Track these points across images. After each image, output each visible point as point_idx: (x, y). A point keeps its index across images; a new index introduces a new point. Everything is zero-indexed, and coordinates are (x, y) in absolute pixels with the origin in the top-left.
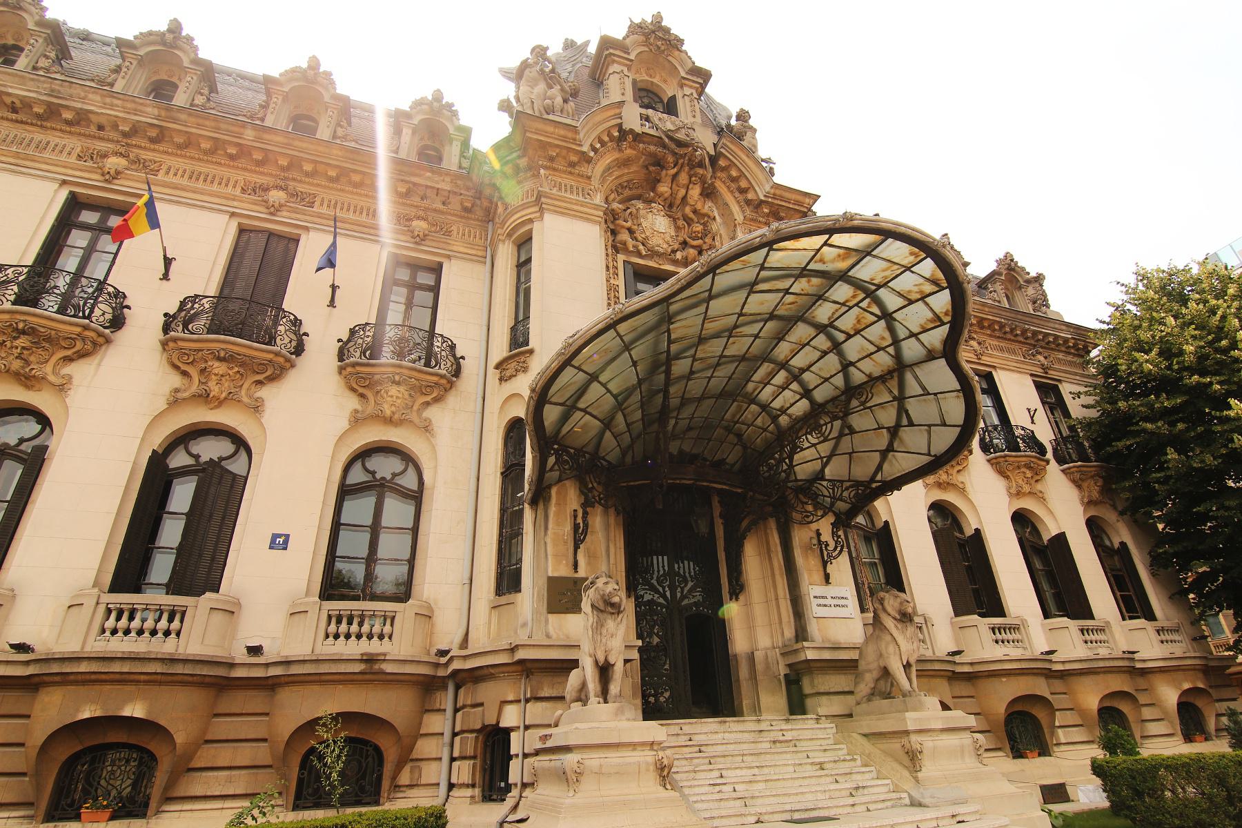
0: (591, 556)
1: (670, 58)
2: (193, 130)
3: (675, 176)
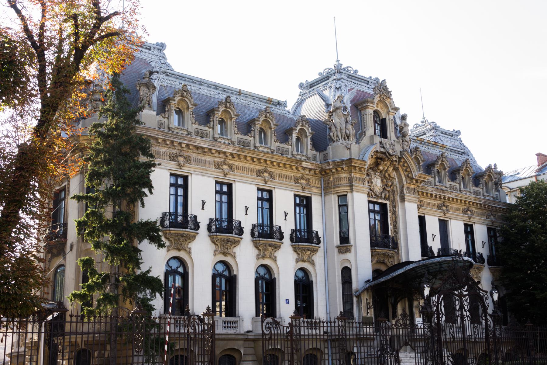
1: (386, 102)
2: (247, 155)
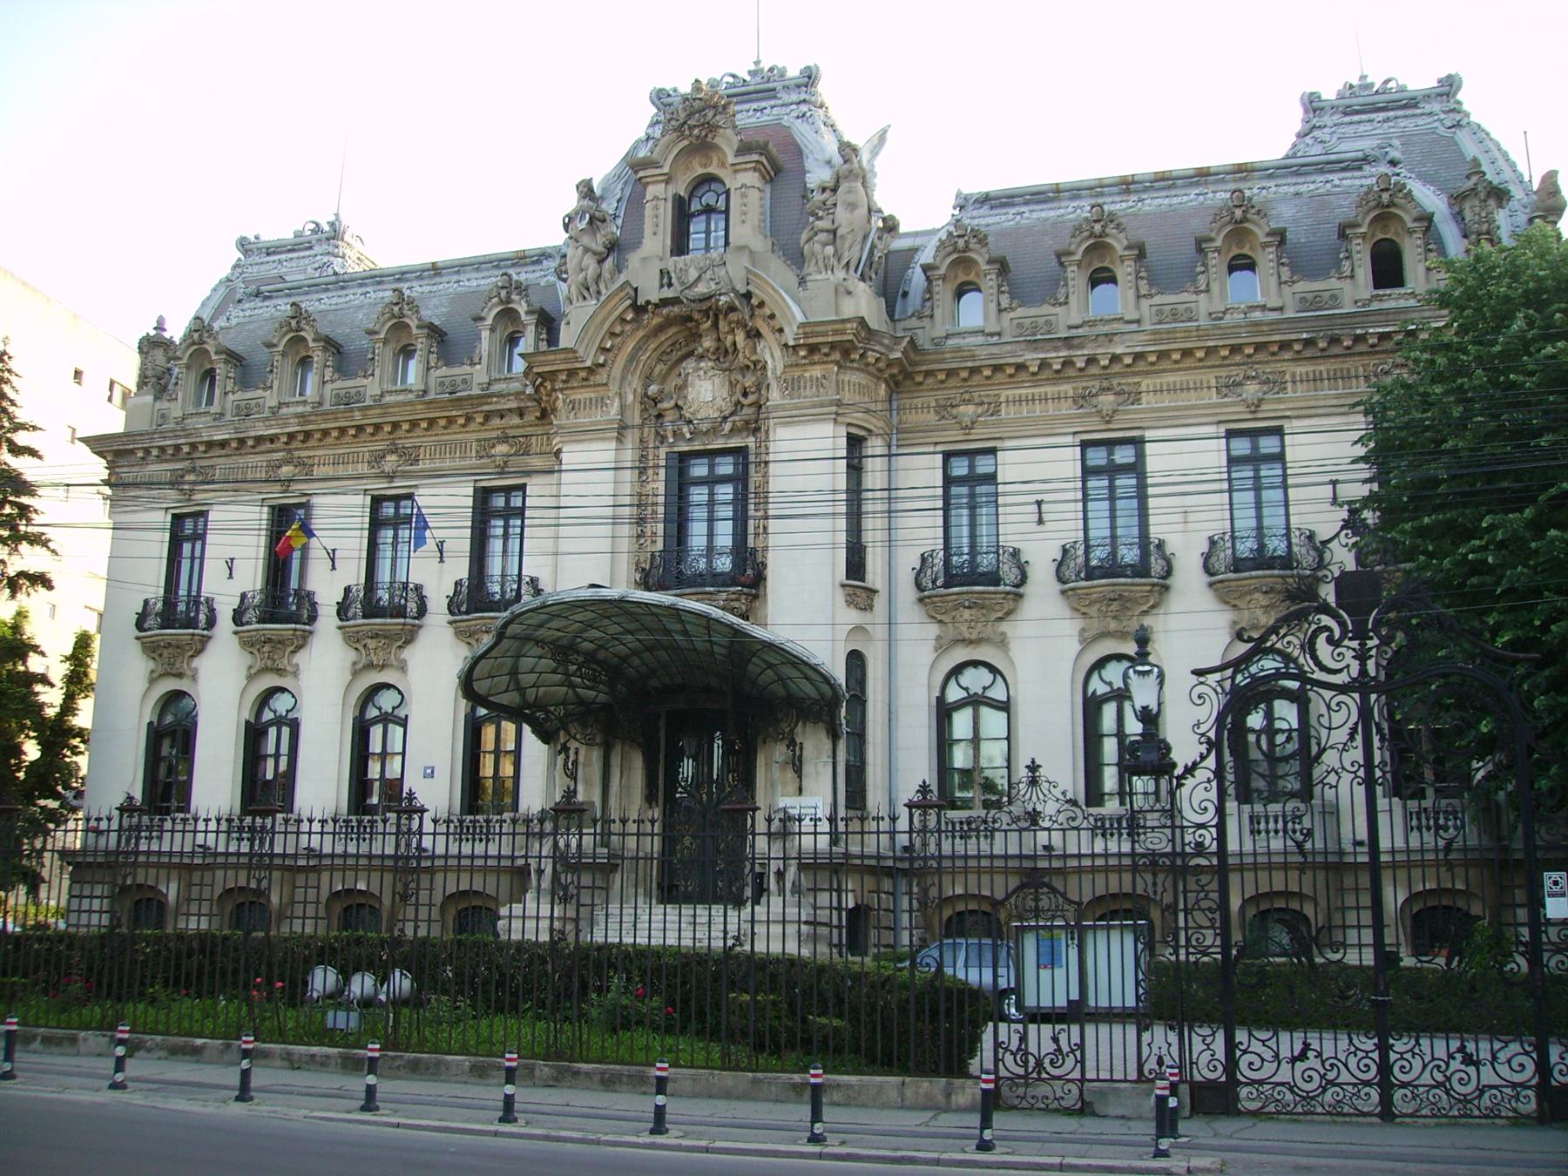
0: (588, 783)
1: (717, 141)
3: (715, 325)
